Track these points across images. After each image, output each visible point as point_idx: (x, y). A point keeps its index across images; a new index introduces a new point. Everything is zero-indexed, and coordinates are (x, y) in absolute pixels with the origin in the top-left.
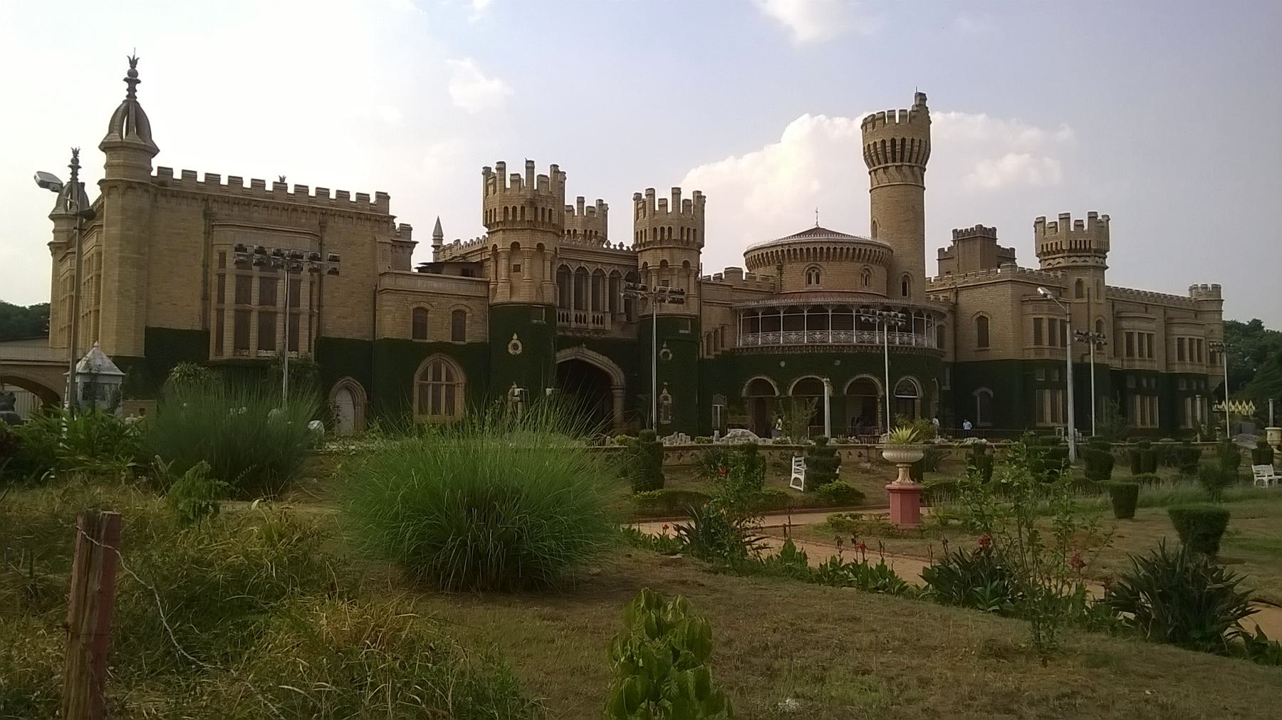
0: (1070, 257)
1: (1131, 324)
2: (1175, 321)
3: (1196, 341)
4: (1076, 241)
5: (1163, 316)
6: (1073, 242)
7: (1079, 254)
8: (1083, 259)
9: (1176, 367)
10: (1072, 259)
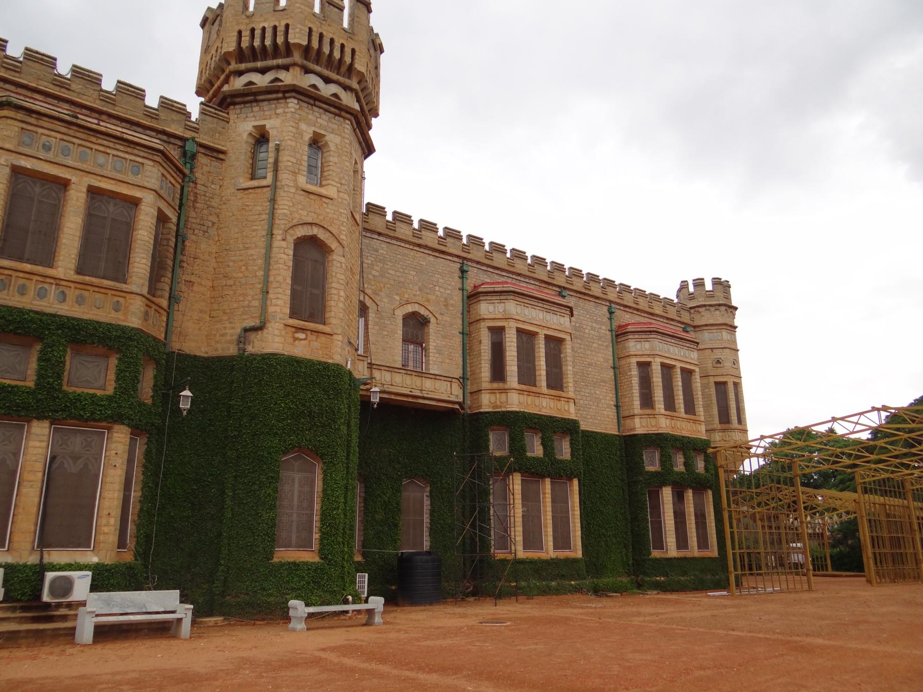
0: (240, 73)
1: (501, 308)
2: (630, 328)
3: (679, 371)
4: (253, 30)
5: (606, 320)
6: (246, 34)
7: (259, 64)
8: (269, 76)
9: (637, 421)
10: (244, 79)
